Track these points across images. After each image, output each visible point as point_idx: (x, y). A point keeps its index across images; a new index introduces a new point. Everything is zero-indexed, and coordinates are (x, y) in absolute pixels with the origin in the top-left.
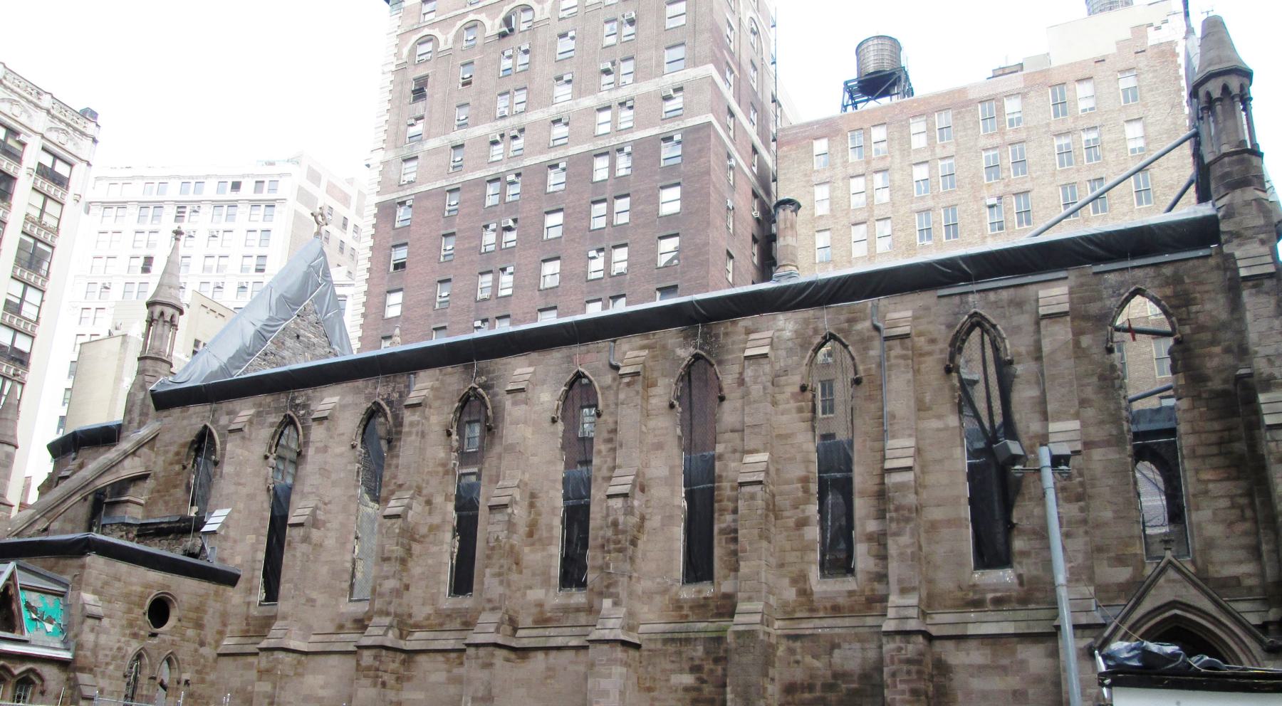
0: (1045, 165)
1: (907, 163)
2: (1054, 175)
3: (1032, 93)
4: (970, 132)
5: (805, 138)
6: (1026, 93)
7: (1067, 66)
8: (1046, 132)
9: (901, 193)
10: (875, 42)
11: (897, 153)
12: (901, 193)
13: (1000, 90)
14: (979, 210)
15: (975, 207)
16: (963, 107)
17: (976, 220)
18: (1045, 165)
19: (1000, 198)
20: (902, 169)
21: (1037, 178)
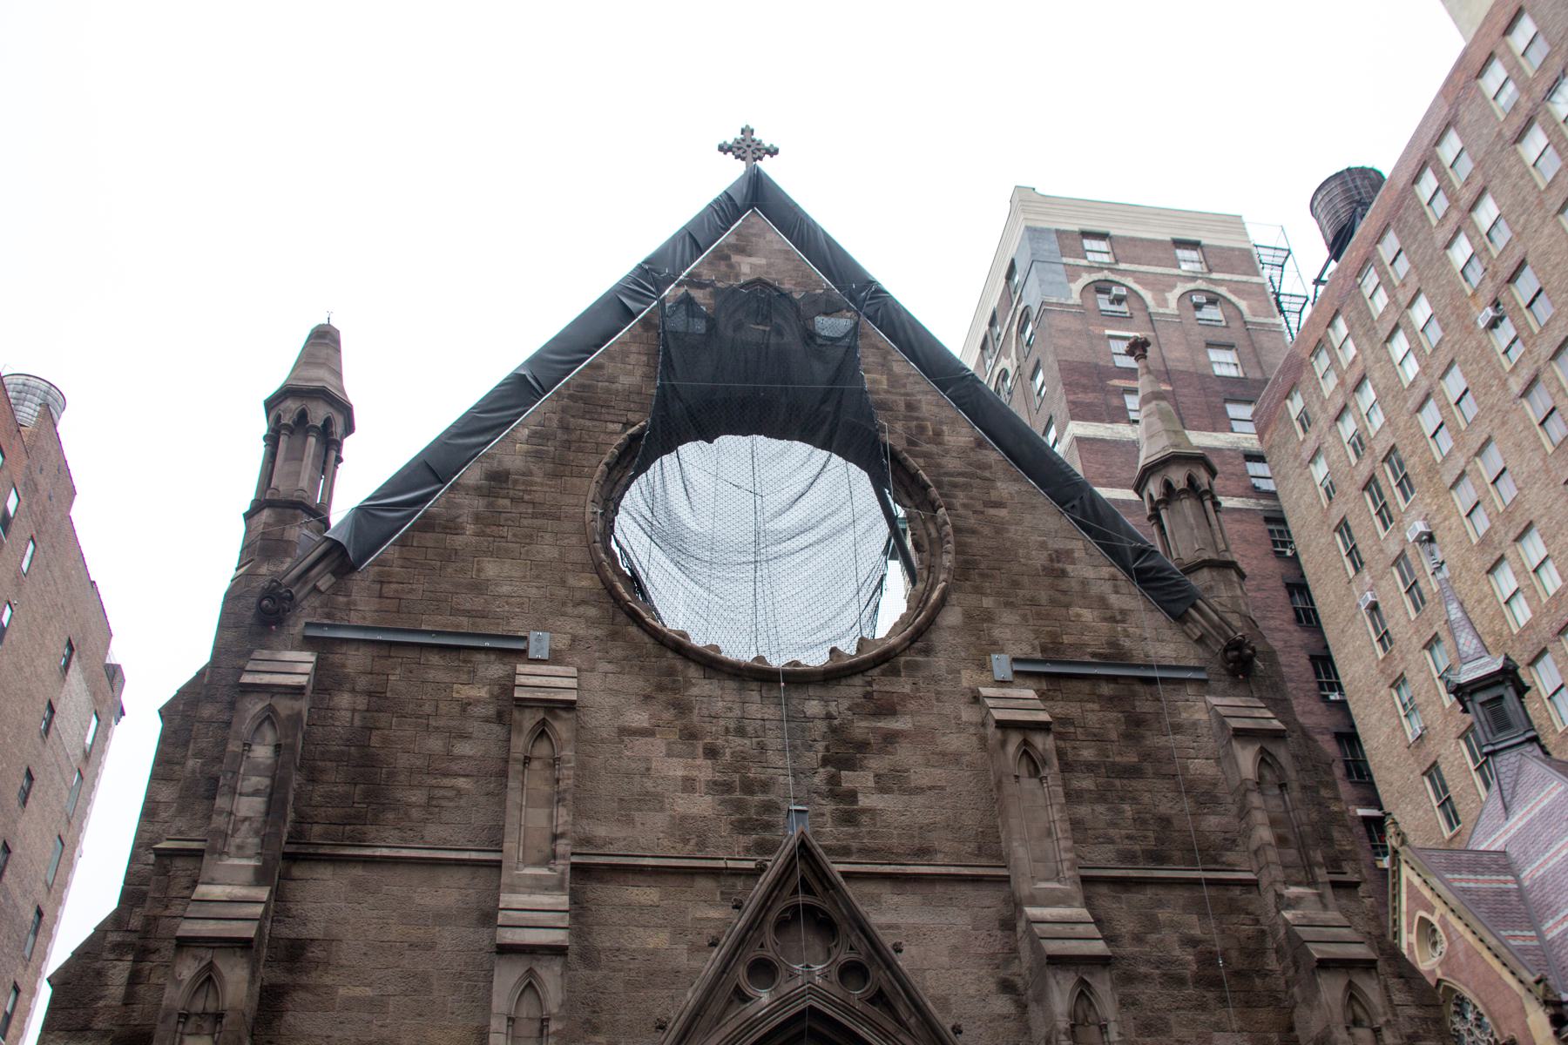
0: (1524, 200)
1: (1379, 346)
2: (1541, 203)
3: (1462, 108)
4: (1421, 237)
5: (1277, 406)
6: (1456, 115)
7: (1483, 25)
8: (1502, 150)
9: (1390, 397)
10: (1319, 197)
11: (1364, 340)
12: (1390, 397)
13: (1426, 142)
14: (1480, 343)
15: (1474, 343)
16: (1399, 208)
17: (1483, 363)
18: (1524, 200)
19: (1496, 304)
20: (1378, 360)
21: (1524, 228)
